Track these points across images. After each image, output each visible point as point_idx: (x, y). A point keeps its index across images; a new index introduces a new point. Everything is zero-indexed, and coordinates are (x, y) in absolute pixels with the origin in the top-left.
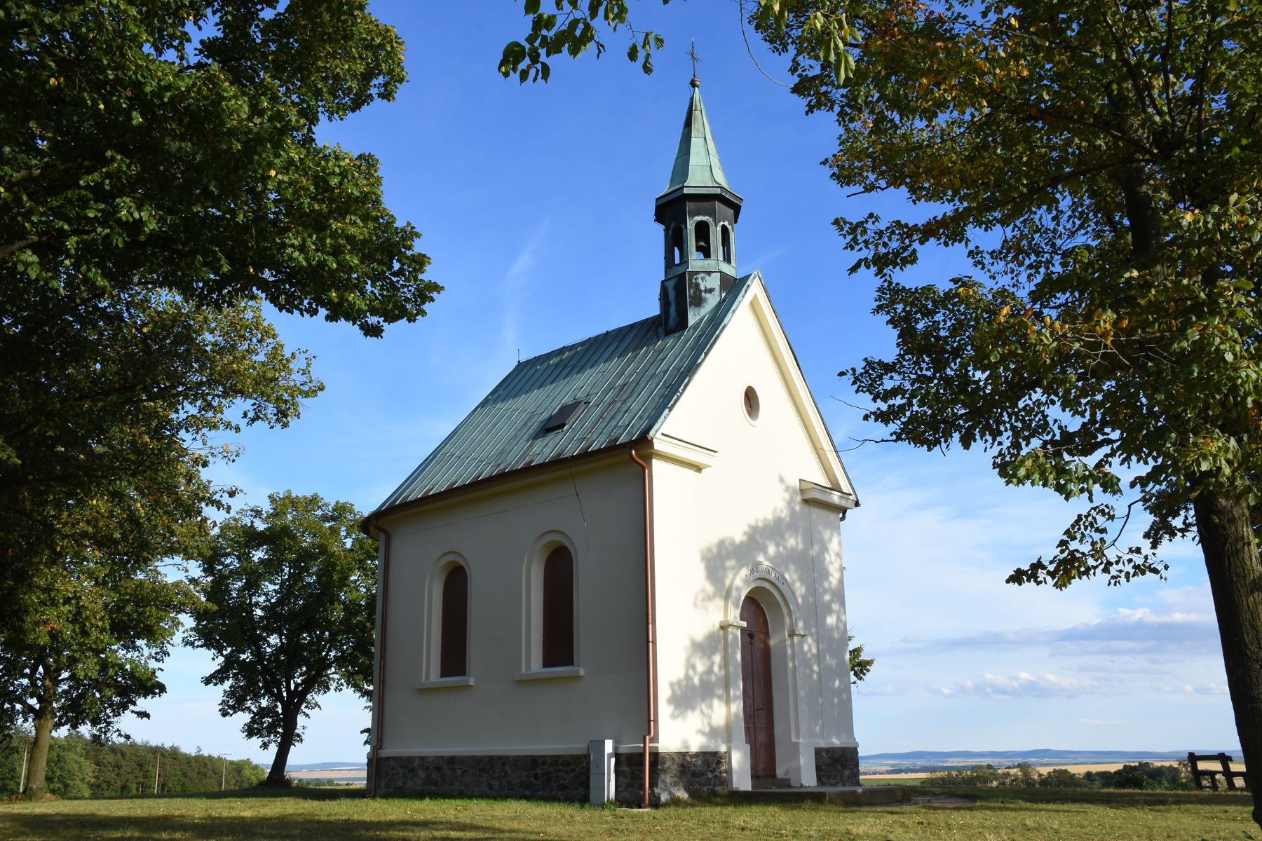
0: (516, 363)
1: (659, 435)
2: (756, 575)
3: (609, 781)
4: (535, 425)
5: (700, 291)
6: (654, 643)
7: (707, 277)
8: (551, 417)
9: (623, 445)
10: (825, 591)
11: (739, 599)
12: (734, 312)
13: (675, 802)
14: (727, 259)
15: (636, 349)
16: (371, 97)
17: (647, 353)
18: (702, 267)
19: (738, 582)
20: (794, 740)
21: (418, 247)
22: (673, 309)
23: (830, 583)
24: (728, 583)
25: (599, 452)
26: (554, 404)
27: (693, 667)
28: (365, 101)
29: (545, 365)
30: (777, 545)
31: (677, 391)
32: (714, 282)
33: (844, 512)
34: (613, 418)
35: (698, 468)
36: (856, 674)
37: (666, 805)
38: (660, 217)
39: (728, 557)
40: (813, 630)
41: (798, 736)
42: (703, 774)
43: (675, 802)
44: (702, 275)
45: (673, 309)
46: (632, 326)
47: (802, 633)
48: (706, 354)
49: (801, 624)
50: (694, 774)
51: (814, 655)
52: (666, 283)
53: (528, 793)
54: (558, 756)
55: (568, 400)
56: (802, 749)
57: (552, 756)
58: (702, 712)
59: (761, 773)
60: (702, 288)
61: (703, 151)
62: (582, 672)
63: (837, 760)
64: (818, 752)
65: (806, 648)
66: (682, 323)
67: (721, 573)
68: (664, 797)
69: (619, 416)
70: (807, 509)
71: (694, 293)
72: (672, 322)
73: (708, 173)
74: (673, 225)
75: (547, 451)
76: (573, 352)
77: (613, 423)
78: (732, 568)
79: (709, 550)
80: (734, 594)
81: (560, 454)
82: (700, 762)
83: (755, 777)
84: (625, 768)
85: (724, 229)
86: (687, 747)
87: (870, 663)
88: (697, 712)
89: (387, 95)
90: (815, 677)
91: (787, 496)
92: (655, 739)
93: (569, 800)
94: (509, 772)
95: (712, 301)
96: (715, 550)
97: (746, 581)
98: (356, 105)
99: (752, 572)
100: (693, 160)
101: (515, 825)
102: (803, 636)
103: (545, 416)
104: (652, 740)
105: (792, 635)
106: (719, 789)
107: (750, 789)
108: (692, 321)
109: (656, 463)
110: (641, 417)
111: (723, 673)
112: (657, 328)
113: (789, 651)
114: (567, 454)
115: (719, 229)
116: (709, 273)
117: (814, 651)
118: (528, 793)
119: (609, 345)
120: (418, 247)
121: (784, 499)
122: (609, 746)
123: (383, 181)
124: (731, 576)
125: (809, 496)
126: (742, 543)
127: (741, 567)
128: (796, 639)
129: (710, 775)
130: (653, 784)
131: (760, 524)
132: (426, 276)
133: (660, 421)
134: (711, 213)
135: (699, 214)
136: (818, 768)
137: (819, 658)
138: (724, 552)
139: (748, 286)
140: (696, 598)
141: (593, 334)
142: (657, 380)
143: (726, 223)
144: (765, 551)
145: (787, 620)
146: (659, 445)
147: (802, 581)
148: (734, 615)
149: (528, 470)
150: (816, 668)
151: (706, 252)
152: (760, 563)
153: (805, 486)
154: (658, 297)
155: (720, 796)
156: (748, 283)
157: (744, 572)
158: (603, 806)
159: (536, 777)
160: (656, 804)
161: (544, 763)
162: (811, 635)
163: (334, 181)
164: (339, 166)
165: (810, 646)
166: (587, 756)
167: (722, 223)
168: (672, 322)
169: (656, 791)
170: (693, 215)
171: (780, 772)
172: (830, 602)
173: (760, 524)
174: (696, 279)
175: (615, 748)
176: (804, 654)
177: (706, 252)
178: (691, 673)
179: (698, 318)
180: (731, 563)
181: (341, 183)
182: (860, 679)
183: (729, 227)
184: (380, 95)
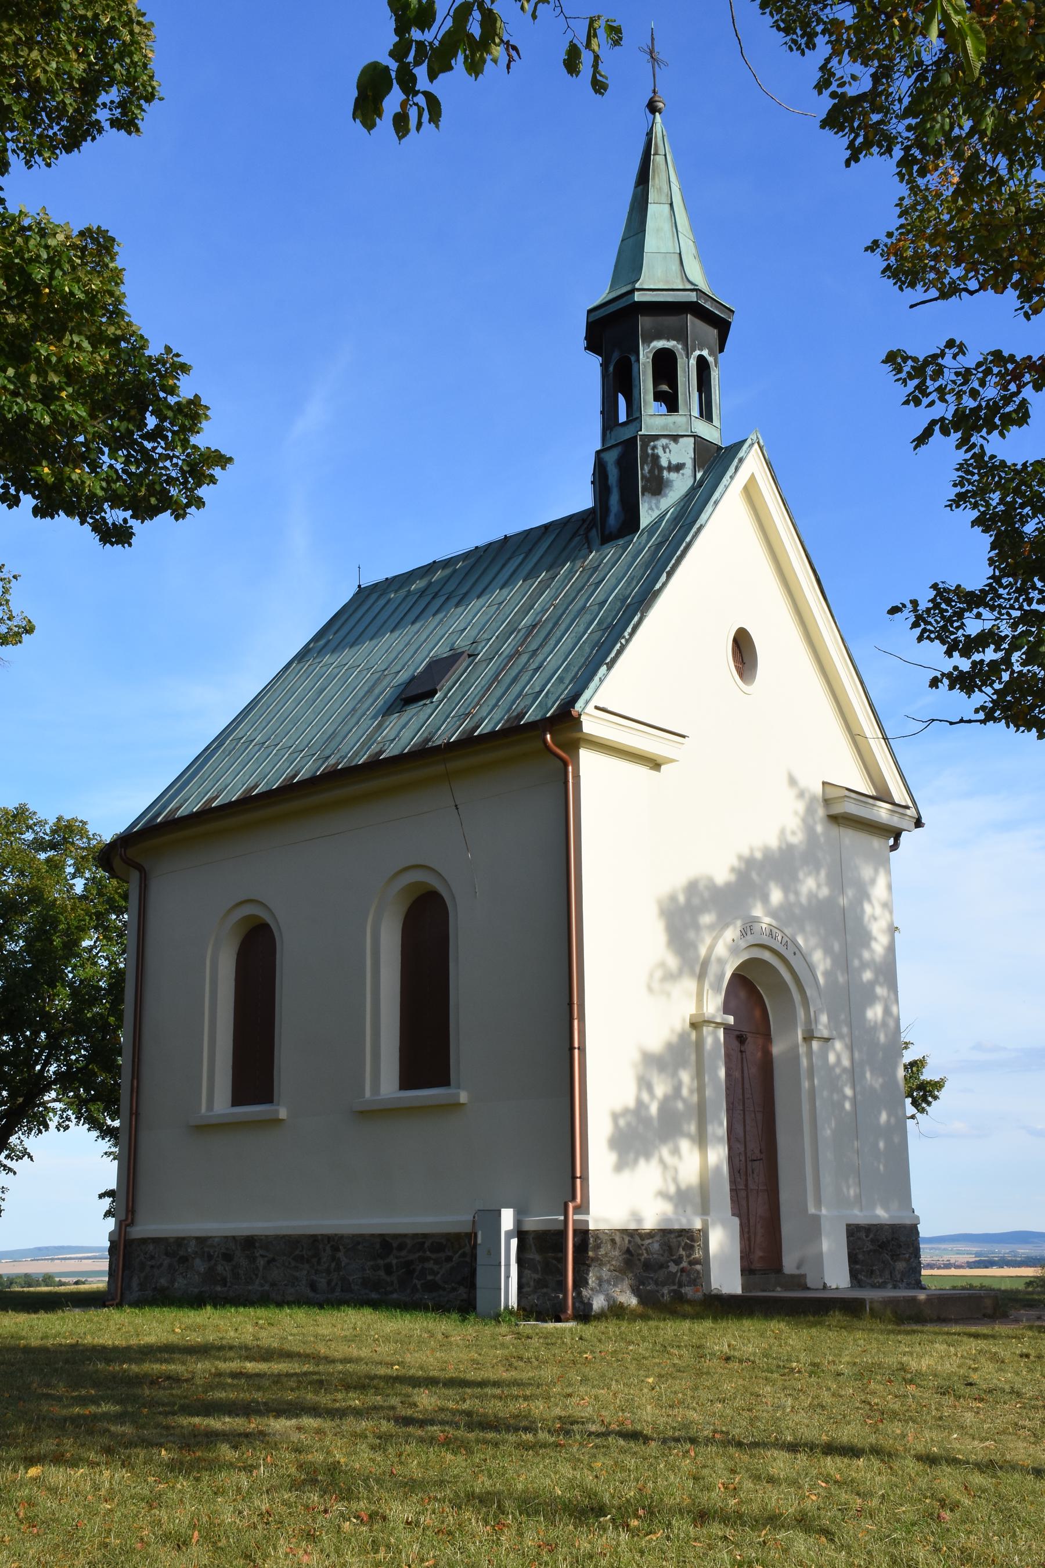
0: (355, 589)
1: (590, 709)
2: (751, 939)
3: (508, 1277)
4: (386, 692)
5: (661, 469)
6: (582, 1049)
8: (413, 679)
9: (532, 725)
10: (864, 966)
11: (723, 975)
12: (716, 503)
13: (617, 1311)
14: (706, 413)
15: (554, 565)
16: (97, 126)
17: (571, 572)
18: (665, 427)
19: (721, 950)
20: (812, 1210)
21: (186, 388)
22: (614, 499)
23: (872, 951)
24: (703, 951)
25: (492, 736)
26: (419, 657)
27: (650, 1088)
28: (87, 133)
29: (403, 592)
30: (786, 889)
31: (620, 635)
32: (683, 453)
33: (897, 835)
34: (515, 680)
35: (655, 764)
36: (915, 1103)
37: (601, 1316)
38: (593, 343)
39: (703, 908)
40: (845, 1030)
41: (818, 1203)
42: (662, 1266)
43: (617, 1311)
44: (664, 441)
45: (614, 499)
46: (546, 528)
47: (826, 1034)
48: (670, 575)
49: (824, 1019)
50: (647, 1266)
51: (845, 1070)
52: (603, 455)
53: (374, 1296)
54: (425, 1236)
55: (440, 650)
56: (825, 1226)
57: (415, 1236)
58: (662, 1161)
59: (757, 1265)
60: (664, 463)
61: (667, 226)
62: (463, 1097)
63: (883, 1246)
64: (856, 1234)
65: (832, 1058)
66: (630, 523)
67: (691, 935)
68: (598, 1303)
69: (525, 678)
70: (835, 831)
71: (651, 471)
72: (612, 521)
73: (675, 267)
74: (616, 356)
75: (406, 734)
76: (448, 571)
77: (516, 689)
78: (711, 927)
79: (673, 898)
80: (713, 969)
81: (427, 740)
82: (656, 1246)
83: (747, 1271)
84: (534, 1256)
85: (702, 362)
86: (639, 1220)
87: (939, 1085)
88: (654, 1162)
89: (127, 123)
90: (848, 1106)
91: (801, 807)
92: (583, 1208)
93: (441, 1308)
94: (344, 1261)
95: (680, 484)
96: (682, 899)
97: (734, 950)
98: (73, 142)
99: (744, 934)
100: (651, 243)
101: (354, 1351)
102: (827, 1040)
103: (404, 676)
104: (578, 1210)
105: (809, 1038)
106: (688, 1291)
107: (738, 1291)
108: (646, 518)
109: (586, 756)
110: (561, 679)
111: (695, 1098)
112: (588, 530)
113: (804, 1062)
114: (439, 740)
115: (693, 362)
116: (675, 438)
117: (846, 1062)
118: (374, 1296)
119: (510, 559)
120: (186, 388)
121: (796, 813)
122: (507, 1219)
123: (126, 277)
124: (708, 941)
125: (838, 809)
126: (728, 885)
127: (726, 926)
128: (815, 1045)
129: (673, 1268)
130: (580, 1281)
131: (758, 855)
132: (203, 440)
133: (592, 686)
134: (680, 335)
135: (659, 337)
136: (853, 1259)
137: (854, 1074)
138: (696, 901)
139: (741, 460)
140: (651, 976)
141: (481, 541)
142: (587, 617)
143: (705, 353)
144: (765, 898)
145: (801, 1013)
146: (591, 725)
147: (828, 950)
148: (713, 1005)
149: (376, 766)
150: (848, 1092)
151: (670, 401)
152: (756, 920)
153: (832, 793)
154: (590, 478)
155: (689, 1302)
156: (741, 454)
157: (730, 934)
158: (497, 1318)
159: (388, 1270)
160: (584, 1315)
161: (401, 1247)
162: (841, 1037)
163: (40, 273)
164: (47, 247)
165: (838, 1054)
166: (471, 1236)
167: (697, 353)
168: (612, 521)
169: (585, 1293)
170: (649, 339)
171: (789, 1264)
172: (872, 984)
173: (758, 855)
174: (654, 448)
175: (518, 1222)
176: (830, 1069)
177: (670, 401)
178: (645, 1097)
179: (656, 514)
181: (52, 276)
182: (922, 1111)
183: (710, 359)
184: (115, 123)
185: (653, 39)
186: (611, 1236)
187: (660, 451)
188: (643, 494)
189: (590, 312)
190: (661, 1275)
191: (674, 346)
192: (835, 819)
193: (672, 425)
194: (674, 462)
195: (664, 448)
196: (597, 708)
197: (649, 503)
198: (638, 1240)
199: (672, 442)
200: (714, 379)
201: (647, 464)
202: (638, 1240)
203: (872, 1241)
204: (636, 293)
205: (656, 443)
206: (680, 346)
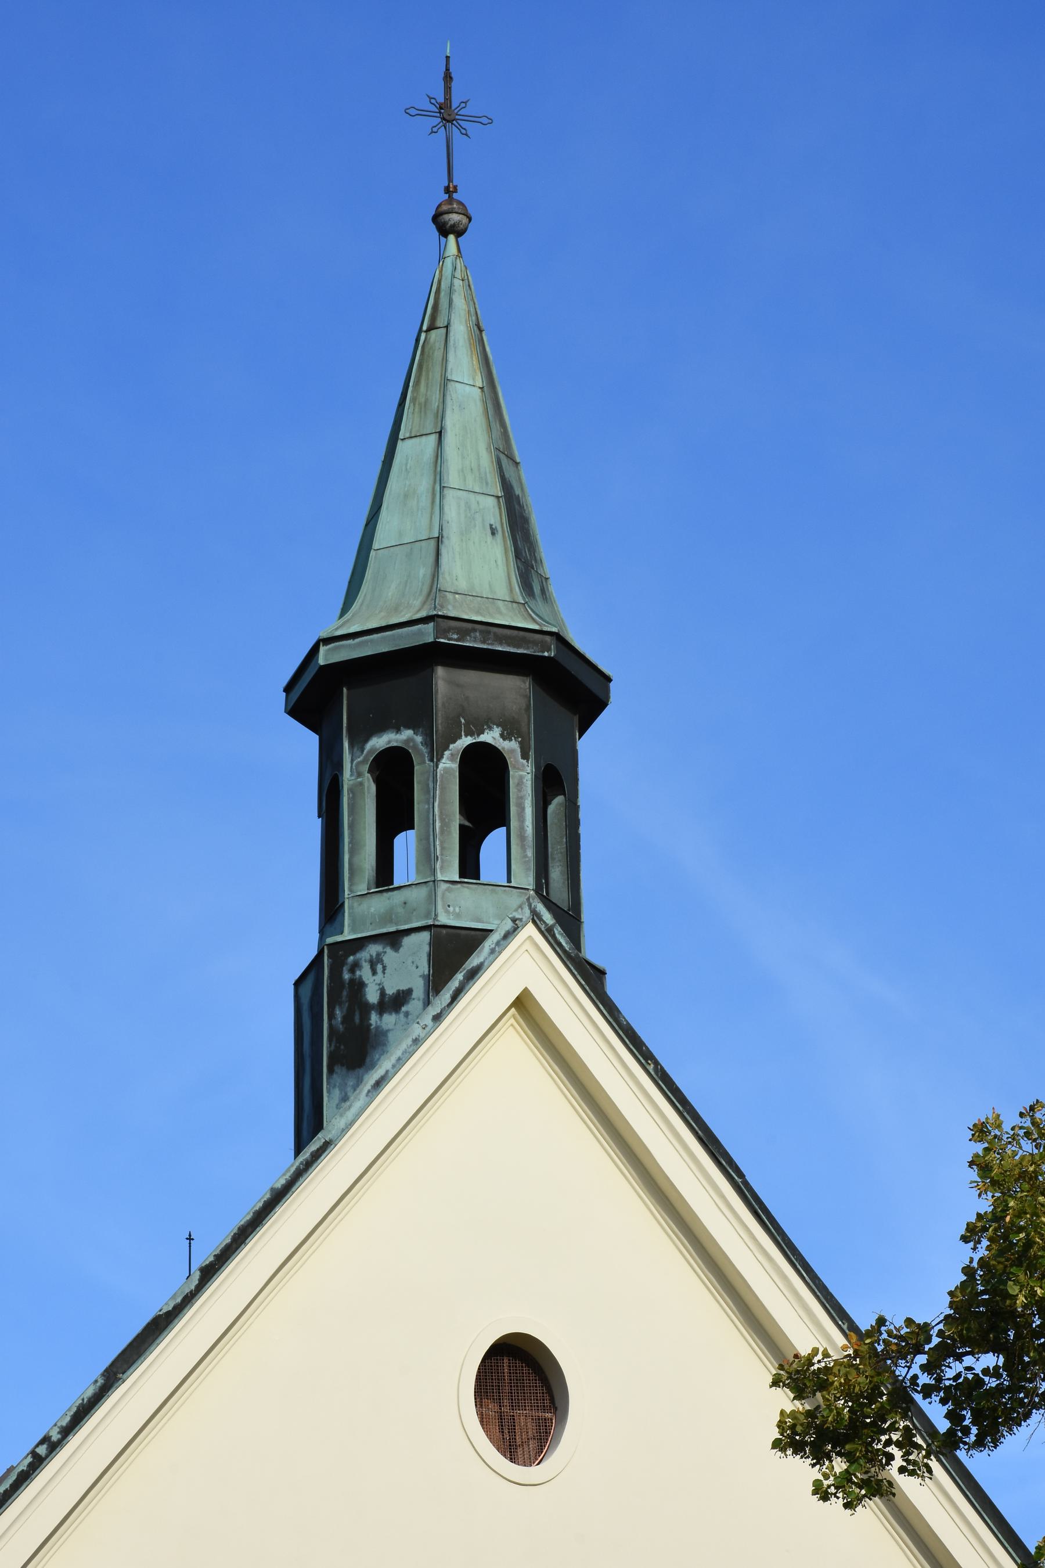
5: (366, 1008)
7: (390, 956)
44: (373, 949)
60: (372, 996)
61: (424, 484)
71: (347, 1019)
115: (449, 764)
116: (394, 939)
135: (380, 729)
139: (473, 974)
143: (491, 736)
156: (474, 961)
174: (356, 966)
185: (448, 77)
187: (365, 973)
188: (331, 1071)
189: (288, 689)
191: (409, 740)
193: (400, 910)
194: (390, 991)
195: (373, 964)
197: (343, 1088)
199: (388, 950)
200: (520, 784)
201: (340, 1004)
204: (322, 649)
205: (358, 955)
206: (419, 739)
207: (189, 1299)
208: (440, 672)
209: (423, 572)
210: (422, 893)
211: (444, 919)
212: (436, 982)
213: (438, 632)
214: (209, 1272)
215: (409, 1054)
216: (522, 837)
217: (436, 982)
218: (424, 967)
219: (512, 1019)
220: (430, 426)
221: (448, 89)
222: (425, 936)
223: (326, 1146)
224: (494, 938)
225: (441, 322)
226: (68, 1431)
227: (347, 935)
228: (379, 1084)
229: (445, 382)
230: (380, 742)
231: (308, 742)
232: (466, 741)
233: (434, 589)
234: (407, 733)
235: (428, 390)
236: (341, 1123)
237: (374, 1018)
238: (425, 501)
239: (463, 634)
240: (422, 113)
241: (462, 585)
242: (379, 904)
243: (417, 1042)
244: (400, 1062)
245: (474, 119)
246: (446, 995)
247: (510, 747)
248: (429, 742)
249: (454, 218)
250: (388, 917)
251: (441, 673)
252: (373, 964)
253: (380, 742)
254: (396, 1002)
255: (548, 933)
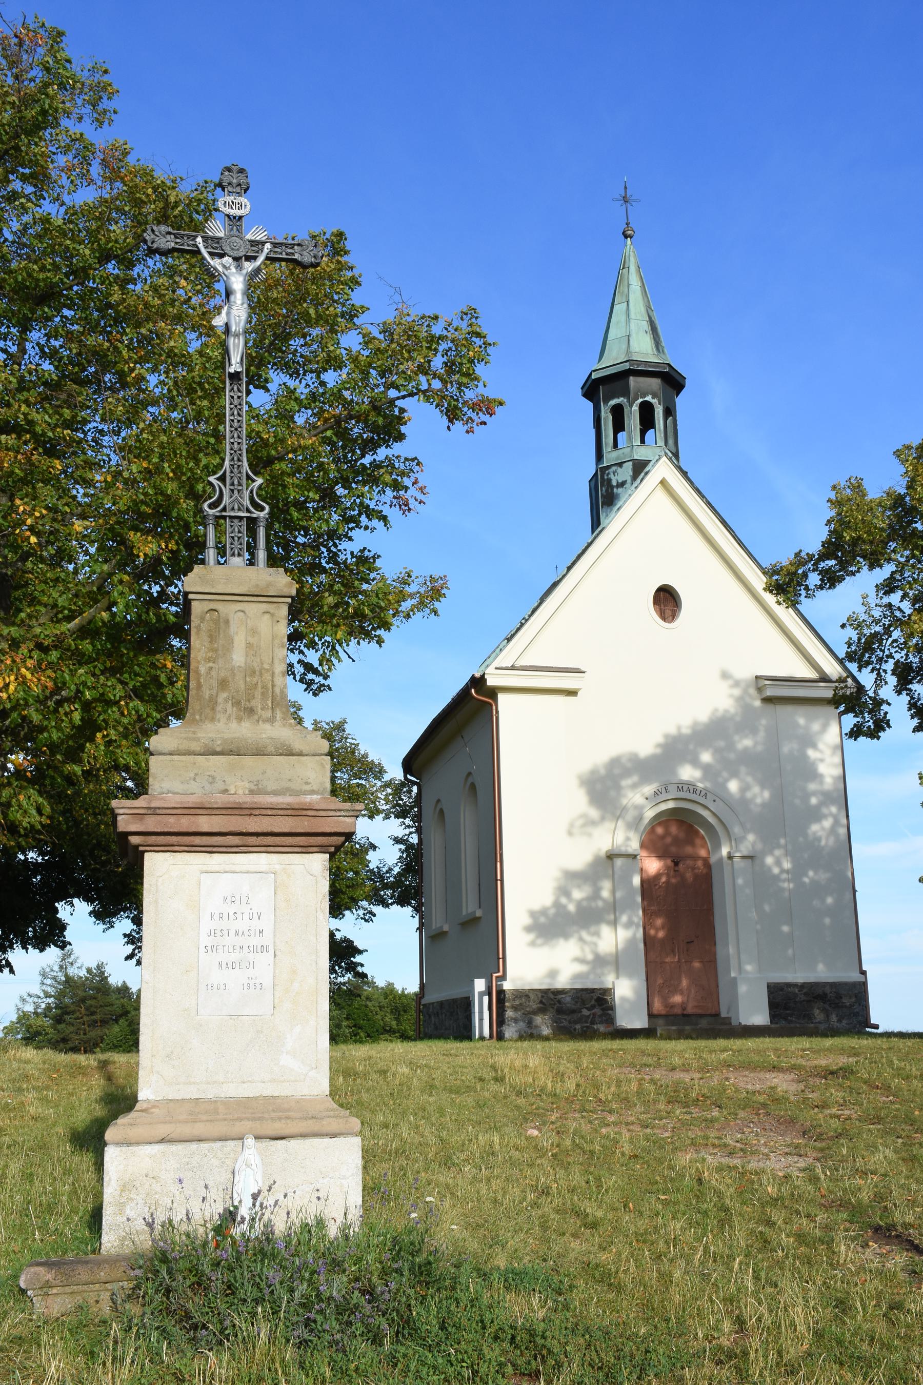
3: (481, 1020)
5: (612, 487)
6: (502, 880)
7: (619, 470)
35: (572, 693)
42: (573, 1011)
44: (614, 468)
60: (614, 483)
61: (623, 318)
70: (770, 707)
71: (607, 491)
82: (568, 999)
92: (503, 977)
115: (635, 408)
116: (620, 465)
129: (585, 1012)
134: (625, 393)
139: (647, 473)
143: (649, 398)
156: (647, 469)
174: (608, 474)
180: (626, 782)
185: (626, 188)
186: (522, 995)
187: (612, 476)
190: (575, 1016)
192: (768, 700)
194: (620, 481)
195: (614, 473)
196: (496, 668)
198: (552, 996)
202: (552, 996)
203: (805, 994)
207: (564, 576)
208: (631, 378)
209: (624, 346)
210: (629, 449)
211: (636, 457)
212: (635, 477)
213: (631, 365)
214: (569, 568)
215: (627, 499)
216: (660, 430)
217: (635, 476)
218: (631, 473)
219: (660, 487)
220: (624, 300)
221: (626, 192)
222: (630, 463)
223: (603, 529)
224: (651, 464)
225: (626, 266)
226: (530, 616)
227: (605, 464)
228: (619, 509)
229: (629, 285)
230: (613, 402)
231: (590, 405)
232: (640, 400)
233: (628, 352)
234: (622, 399)
235: (622, 288)
236: (607, 521)
237: (615, 490)
238: (624, 324)
239: (638, 365)
240: (618, 200)
241: (637, 350)
242: (615, 454)
243: (630, 495)
244: (625, 502)
245: (635, 200)
246: (639, 480)
247: (654, 401)
248: (629, 401)
249: (629, 232)
250: (618, 458)
251: (632, 379)
252: (614, 473)
253: (613, 402)
254: (622, 484)
255: (670, 459)
